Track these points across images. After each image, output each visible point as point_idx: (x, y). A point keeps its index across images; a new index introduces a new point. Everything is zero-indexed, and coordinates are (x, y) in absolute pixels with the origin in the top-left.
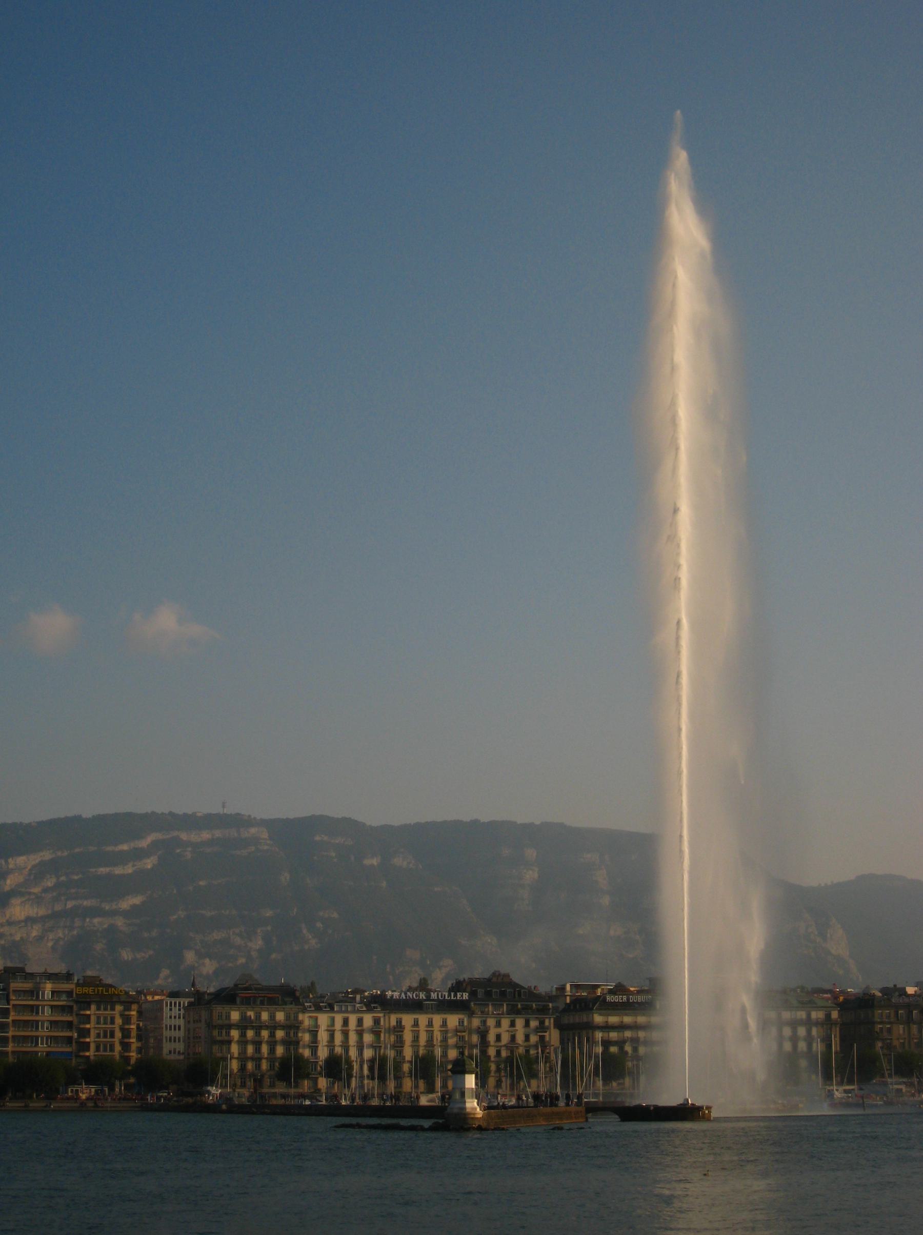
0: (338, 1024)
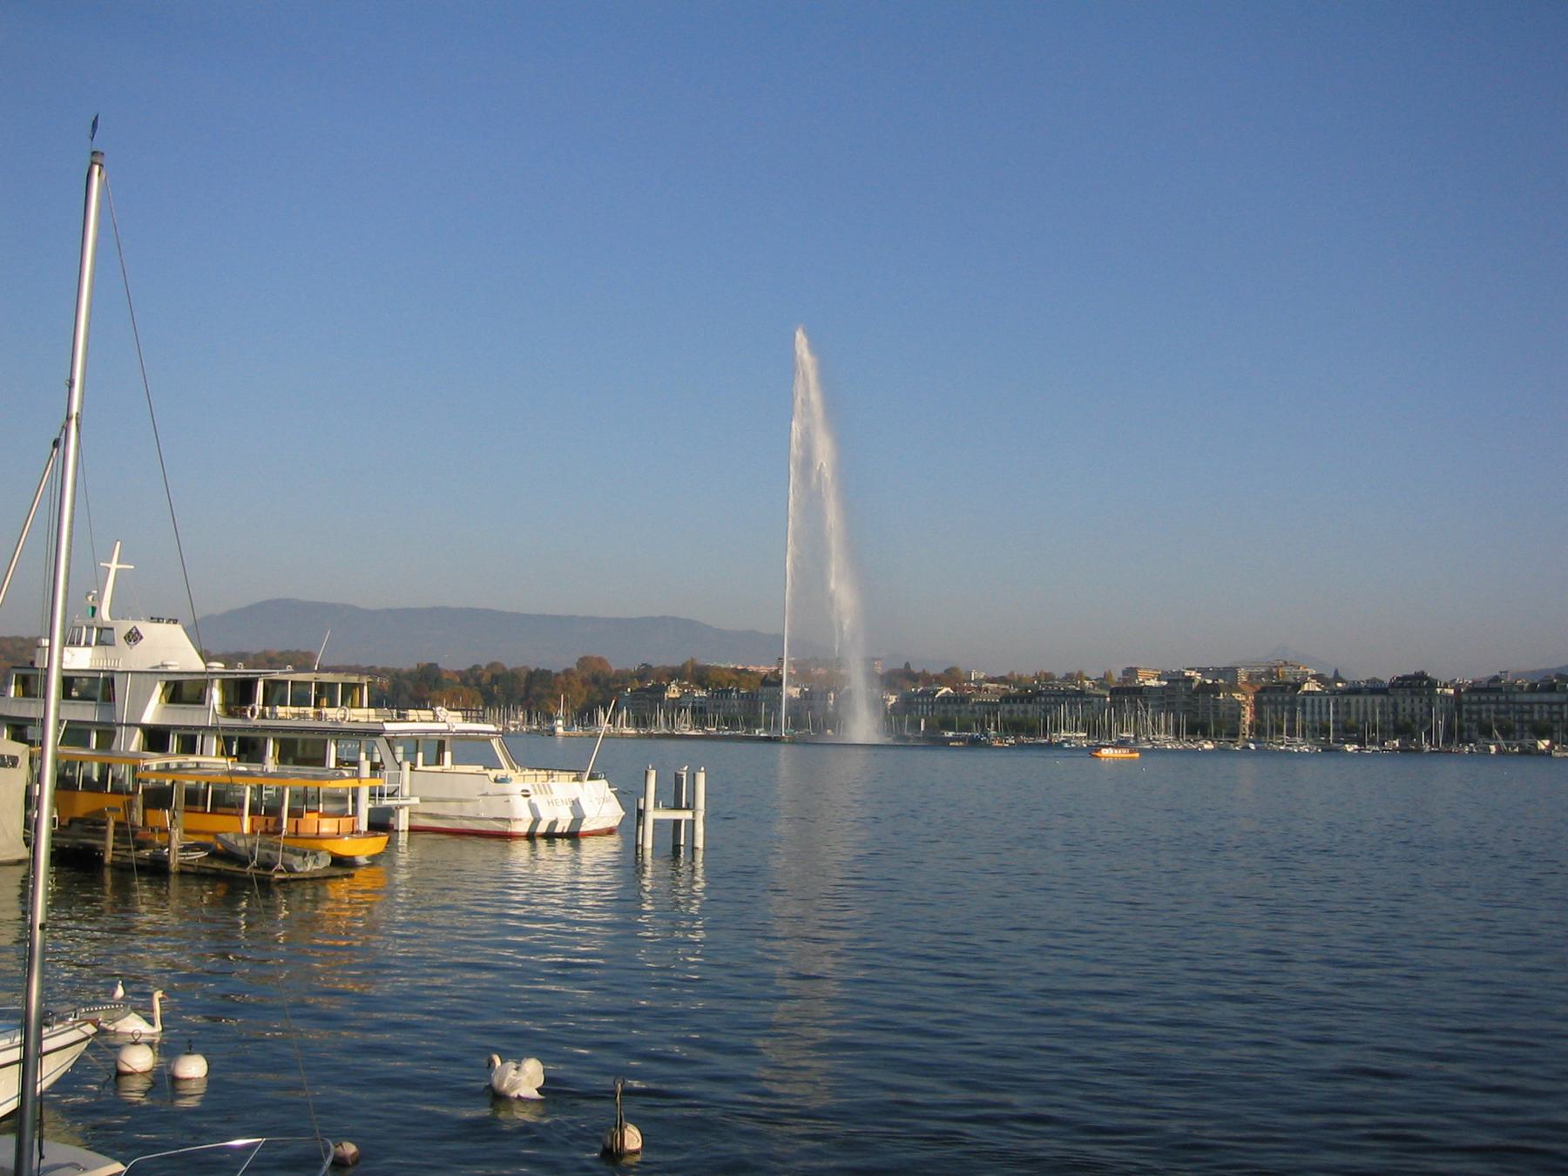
0: (1316, 703)
